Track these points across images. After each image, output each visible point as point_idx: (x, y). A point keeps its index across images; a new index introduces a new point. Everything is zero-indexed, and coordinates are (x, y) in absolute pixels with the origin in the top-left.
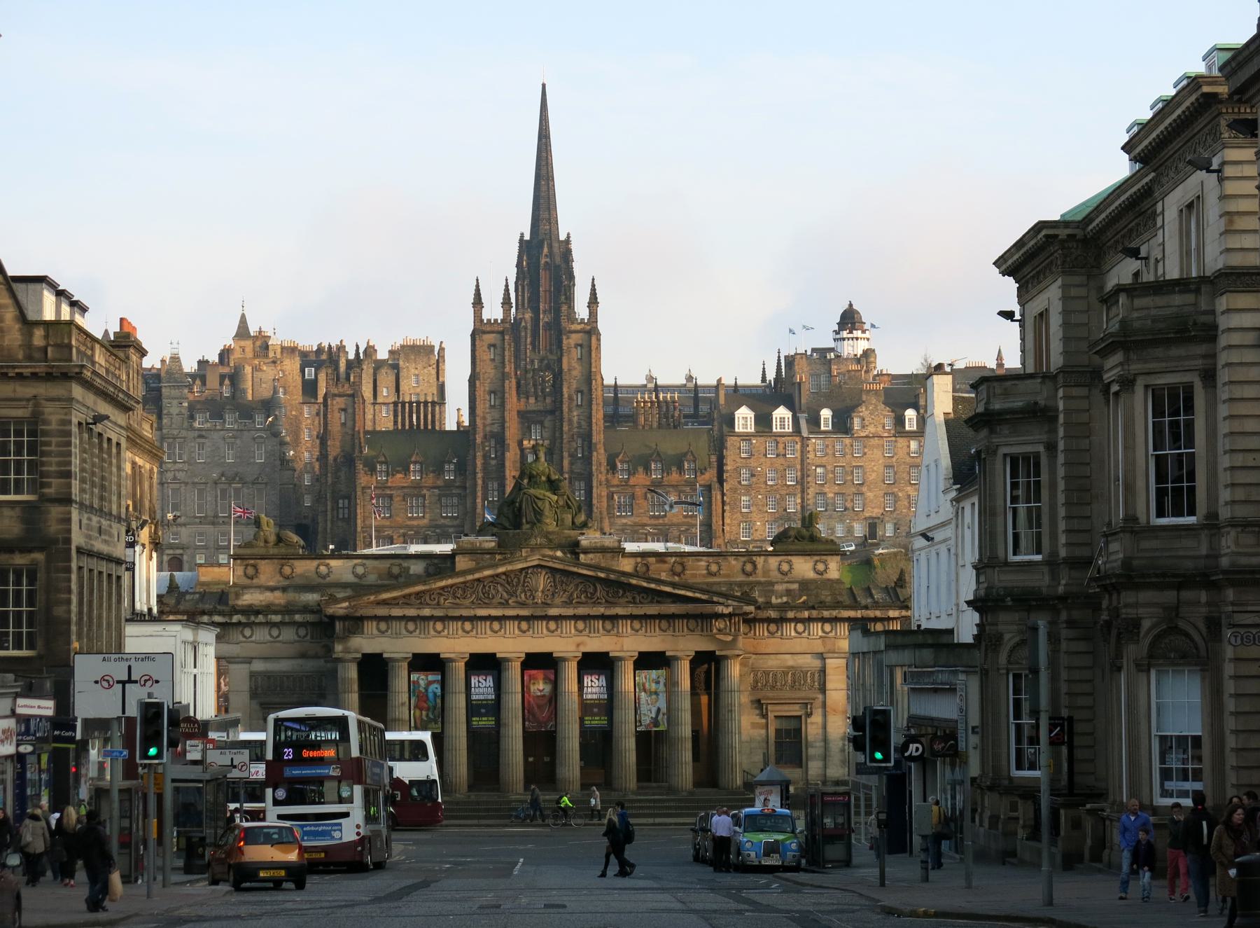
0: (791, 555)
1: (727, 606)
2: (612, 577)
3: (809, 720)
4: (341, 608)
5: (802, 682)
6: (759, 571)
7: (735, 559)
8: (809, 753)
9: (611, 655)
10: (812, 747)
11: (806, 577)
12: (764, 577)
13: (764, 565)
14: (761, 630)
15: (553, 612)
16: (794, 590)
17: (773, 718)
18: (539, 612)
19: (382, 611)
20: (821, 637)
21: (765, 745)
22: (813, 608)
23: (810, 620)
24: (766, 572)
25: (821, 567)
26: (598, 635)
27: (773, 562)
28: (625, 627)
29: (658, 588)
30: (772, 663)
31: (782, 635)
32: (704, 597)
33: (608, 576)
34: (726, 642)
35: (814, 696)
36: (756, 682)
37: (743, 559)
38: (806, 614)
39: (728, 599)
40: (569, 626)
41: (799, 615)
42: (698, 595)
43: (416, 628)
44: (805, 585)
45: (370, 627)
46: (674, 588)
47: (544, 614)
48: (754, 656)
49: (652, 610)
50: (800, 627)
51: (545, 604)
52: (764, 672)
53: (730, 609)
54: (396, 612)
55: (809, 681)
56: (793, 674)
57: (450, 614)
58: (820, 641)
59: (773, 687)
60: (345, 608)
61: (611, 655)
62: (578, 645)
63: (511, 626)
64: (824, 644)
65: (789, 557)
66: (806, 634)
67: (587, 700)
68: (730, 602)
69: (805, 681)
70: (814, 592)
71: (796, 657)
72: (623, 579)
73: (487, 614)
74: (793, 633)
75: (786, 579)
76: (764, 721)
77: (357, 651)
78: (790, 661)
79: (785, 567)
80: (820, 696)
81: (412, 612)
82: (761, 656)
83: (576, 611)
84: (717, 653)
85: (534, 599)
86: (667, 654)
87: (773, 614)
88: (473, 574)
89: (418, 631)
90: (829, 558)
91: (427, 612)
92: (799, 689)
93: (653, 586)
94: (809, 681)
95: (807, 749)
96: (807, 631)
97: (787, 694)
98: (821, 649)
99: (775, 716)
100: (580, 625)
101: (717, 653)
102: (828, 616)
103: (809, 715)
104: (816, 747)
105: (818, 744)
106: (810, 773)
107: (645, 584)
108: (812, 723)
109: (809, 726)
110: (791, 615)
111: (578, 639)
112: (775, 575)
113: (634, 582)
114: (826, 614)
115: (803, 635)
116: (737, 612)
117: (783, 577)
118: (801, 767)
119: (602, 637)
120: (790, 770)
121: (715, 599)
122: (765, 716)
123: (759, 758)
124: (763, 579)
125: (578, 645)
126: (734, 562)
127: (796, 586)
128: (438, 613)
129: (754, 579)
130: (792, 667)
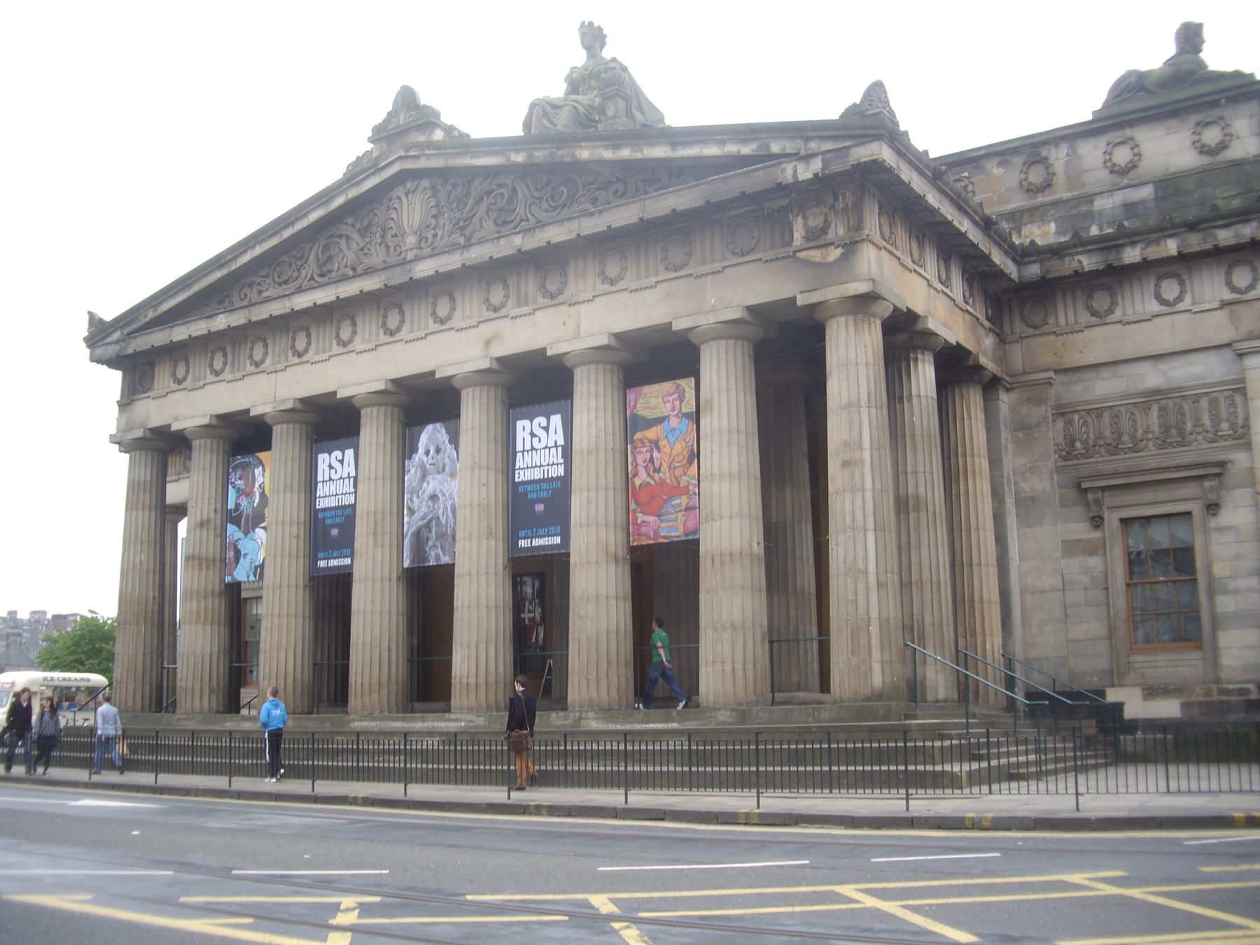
0: (1131, 124)
1: (807, 158)
2: (539, 155)
3: (1213, 523)
4: (110, 343)
5: (1189, 425)
6: (1060, 180)
7: (1000, 164)
8: (1220, 610)
9: (549, 353)
10: (1226, 592)
11: (1173, 169)
12: (1070, 189)
13: (1067, 163)
14: (1067, 313)
15: (424, 269)
16: (1143, 202)
17: (1116, 523)
18: (398, 277)
19: (158, 338)
20: (1224, 305)
21: (1100, 595)
22: (1192, 227)
23: (1187, 262)
24: (1074, 177)
25: (1212, 136)
26: (525, 310)
27: (1092, 153)
28: (582, 282)
29: (639, 156)
30: (1104, 387)
31: (1124, 314)
32: (746, 150)
33: (530, 156)
34: (827, 265)
35: (1221, 457)
36: (1071, 441)
37: (1018, 161)
38: (1171, 247)
39: (807, 139)
40: (469, 306)
41: (1154, 253)
42: (732, 148)
43: (225, 363)
44: (1169, 185)
45: (163, 378)
46: (674, 145)
47: (405, 279)
48: (1061, 378)
49: (625, 215)
50: (1170, 289)
51: (418, 259)
52: (1088, 411)
53: (817, 165)
54: (180, 333)
55: (1206, 420)
56: (1162, 409)
57: (254, 319)
58: (1222, 315)
59: (1114, 449)
60: (117, 342)
61: (549, 353)
62: (488, 343)
63: (368, 328)
64: (1234, 320)
65: (1128, 132)
66: (1186, 304)
67: (523, 483)
68: (813, 146)
69: (1198, 423)
70: (1196, 196)
71: (1164, 366)
72: (564, 155)
73: (310, 304)
74: (1155, 307)
75: (1126, 182)
76: (1097, 534)
77: (141, 425)
78: (1151, 377)
79: (1122, 156)
80: (1240, 459)
81: (199, 328)
82: (1075, 377)
83: (466, 255)
84: (800, 301)
85: (400, 254)
86: (679, 325)
87: (1088, 262)
88: (293, 223)
89: (228, 369)
90: (1228, 112)
91: (221, 322)
92: (1180, 444)
93: (626, 153)
94: (1206, 420)
95: (1211, 598)
96: (1188, 298)
97: (1152, 457)
98: (1226, 335)
99: (1125, 522)
100: (497, 296)
101: (799, 302)
102: (1232, 242)
103: (1213, 508)
104: (1236, 591)
105: (1241, 584)
106: (1226, 661)
107: (608, 155)
108: (1221, 530)
109: (1215, 537)
110: (1132, 255)
111: (487, 329)
112: (1097, 176)
113: (584, 154)
114: (1225, 237)
115: (1180, 306)
116: (836, 168)
117: (1116, 179)
118: (1200, 648)
119: (538, 313)
120: (1170, 656)
121: (775, 148)
122: (1097, 521)
123: (1091, 627)
124: (1065, 195)
125: (488, 343)
126: (997, 171)
127: (1147, 192)
128: (237, 319)
129: (1048, 199)
130: (1158, 391)
